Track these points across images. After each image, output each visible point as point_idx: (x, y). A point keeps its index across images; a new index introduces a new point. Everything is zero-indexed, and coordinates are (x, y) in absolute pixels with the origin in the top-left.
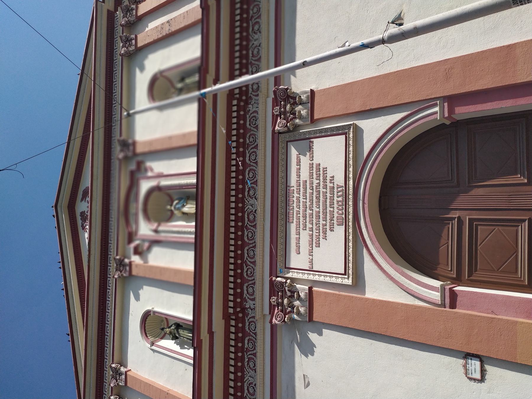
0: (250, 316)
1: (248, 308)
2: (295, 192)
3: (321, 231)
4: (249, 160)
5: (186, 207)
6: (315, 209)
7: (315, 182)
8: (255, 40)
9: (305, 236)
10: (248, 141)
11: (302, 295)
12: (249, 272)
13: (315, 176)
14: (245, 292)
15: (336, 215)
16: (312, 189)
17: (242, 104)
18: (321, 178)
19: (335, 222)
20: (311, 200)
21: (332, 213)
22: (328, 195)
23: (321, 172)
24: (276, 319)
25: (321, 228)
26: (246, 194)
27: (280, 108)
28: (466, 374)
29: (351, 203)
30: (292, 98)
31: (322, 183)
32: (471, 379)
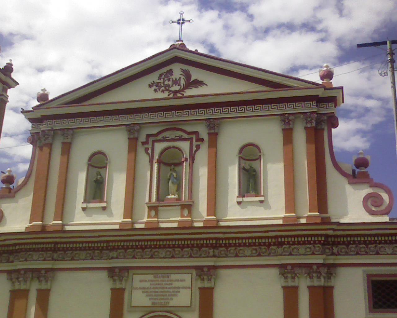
6: (159, 290)
7: (171, 290)
9: (147, 285)
14: (120, 251)
17: (214, 245)
18: (173, 293)
19: (153, 301)
20: (163, 288)
21: (157, 299)
22: (165, 297)
23: (176, 294)
29: (161, 309)
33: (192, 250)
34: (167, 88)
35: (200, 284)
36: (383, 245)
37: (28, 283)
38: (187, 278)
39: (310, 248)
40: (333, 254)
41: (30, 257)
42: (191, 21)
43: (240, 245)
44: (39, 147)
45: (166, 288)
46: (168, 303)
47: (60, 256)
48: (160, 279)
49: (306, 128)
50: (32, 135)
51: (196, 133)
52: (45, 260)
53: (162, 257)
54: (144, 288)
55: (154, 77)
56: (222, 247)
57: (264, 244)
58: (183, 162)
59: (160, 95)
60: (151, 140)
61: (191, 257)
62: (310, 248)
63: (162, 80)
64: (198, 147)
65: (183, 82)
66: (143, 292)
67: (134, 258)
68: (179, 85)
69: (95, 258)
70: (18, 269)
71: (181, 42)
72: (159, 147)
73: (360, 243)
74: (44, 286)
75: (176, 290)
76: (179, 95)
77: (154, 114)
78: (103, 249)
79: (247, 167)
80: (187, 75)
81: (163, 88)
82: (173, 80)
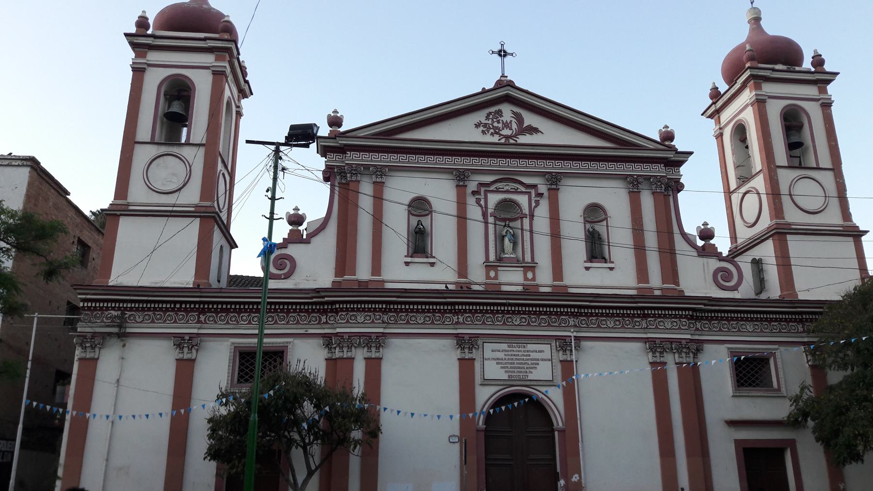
3: (505, 365)
4: (542, 318)
5: (509, 243)
6: (515, 362)
7: (529, 362)
8: (610, 322)
9: (501, 355)
10: (553, 317)
12: (479, 318)
13: (533, 362)
14: (467, 315)
15: (513, 374)
17: (575, 314)
20: (519, 359)
22: (524, 370)
23: (535, 366)
25: (506, 365)
28: (451, 436)
29: (519, 383)
33: (550, 318)
34: (497, 131)
35: (562, 357)
36: (744, 323)
37: (353, 349)
38: (546, 348)
39: (676, 322)
40: (697, 329)
42: (514, 55)
43: (602, 315)
45: (523, 360)
46: (527, 376)
47: (392, 319)
48: (514, 349)
49: (653, 193)
50: (328, 166)
51: (534, 186)
52: (373, 322)
53: (517, 324)
54: (498, 359)
55: (480, 116)
57: (628, 315)
58: (522, 218)
59: (488, 138)
60: (483, 189)
61: (549, 325)
62: (676, 322)
63: (490, 120)
64: (537, 203)
65: (514, 126)
66: (497, 363)
67: (484, 323)
68: (511, 129)
69: (435, 323)
70: (337, 333)
71: (505, 78)
72: (494, 199)
73: (722, 318)
74: (374, 355)
76: (511, 141)
78: (445, 311)
79: (591, 230)
80: (519, 119)
81: (492, 131)
82: (503, 123)
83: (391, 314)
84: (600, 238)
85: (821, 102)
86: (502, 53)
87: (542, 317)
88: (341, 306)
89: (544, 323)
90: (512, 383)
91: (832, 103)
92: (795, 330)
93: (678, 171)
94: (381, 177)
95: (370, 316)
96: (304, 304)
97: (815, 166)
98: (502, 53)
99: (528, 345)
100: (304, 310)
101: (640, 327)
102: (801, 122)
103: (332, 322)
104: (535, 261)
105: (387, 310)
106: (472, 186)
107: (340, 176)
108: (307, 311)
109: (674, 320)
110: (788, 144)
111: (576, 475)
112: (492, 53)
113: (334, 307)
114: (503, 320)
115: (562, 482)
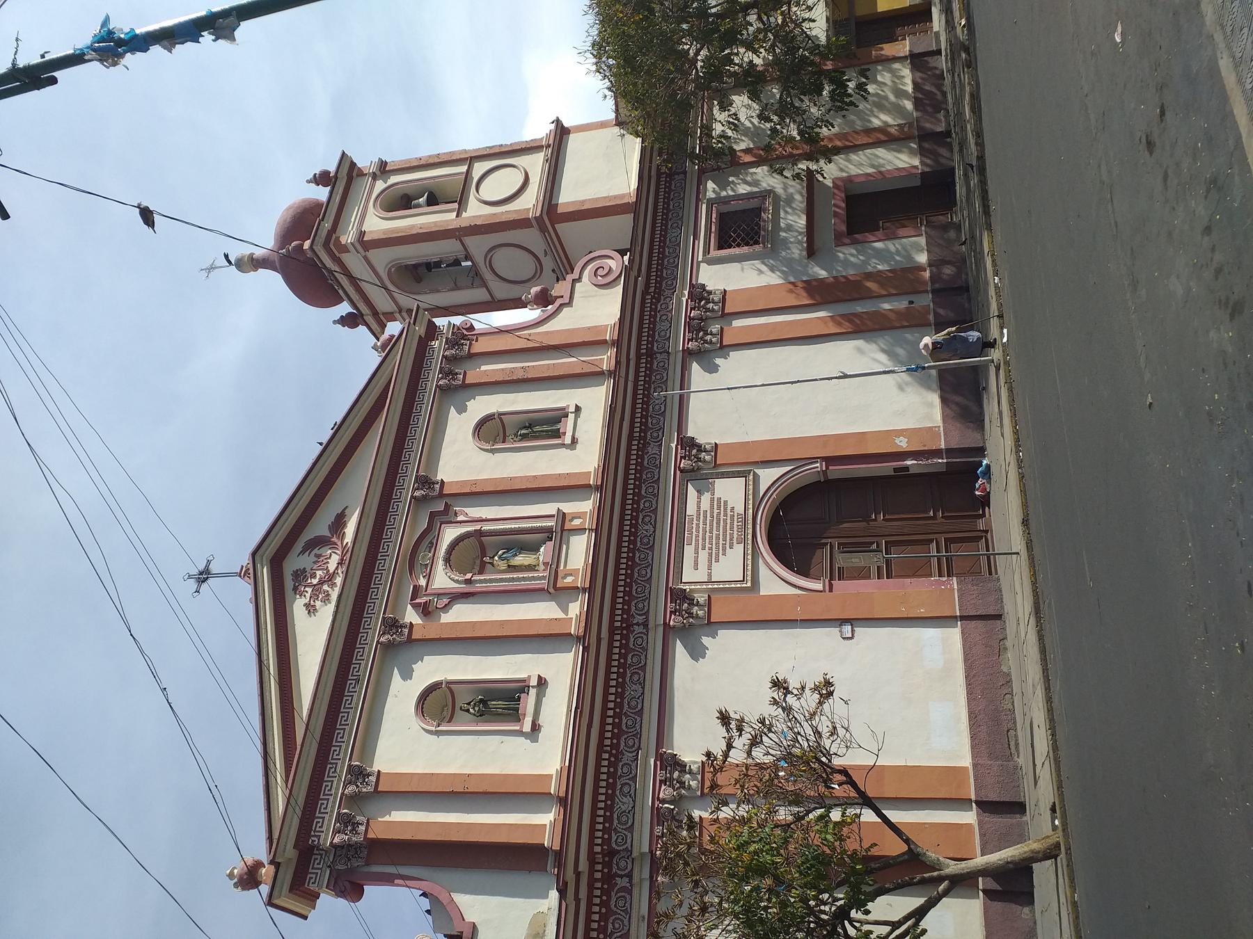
0: (635, 632)
1: (635, 624)
2: (695, 520)
6: (715, 532)
7: (716, 511)
9: (703, 555)
10: (644, 477)
11: (701, 600)
13: (715, 506)
16: (713, 517)
17: (641, 445)
18: (722, 509)
20: (711, 525)
21: (732, 535)
22: (729, 521)
24: (675, 622)
26: (640, 521)
27: (685, 452)
29: (750, 526)
30: (696, 446)
31: (722, 514)
32: (843, 638)
41: (624, 818)
42: (211, 558)
44: (368, 865)
46: (738, 514)
48: (694, 533)
49: (471, 356)
51: (433, 515)
53: (652, 529)
54: (710, 561)
56: (645, 437)
63: (307, 589)
66: (717, 561)
69: (643, 663)
70: (651, 852)
72: (443, 579)
75: (715, 503)
77: (376, 577)
83: (622, 744)
84: (530, 426)
85: (378, 173)
86: (204, 576)
87: (643, 492)
88: (599, 841)
89: (654, 489)
90: (750, 537)
91: (382, 161)
92: (681, 183)
93: (442, 328)
94: (369, 775)
95: (623, 785)
96: (588, 920)
97: (464, 176)
98: (204, 576)
99: (687, 514)
100: (602, 924)
101: (667, 361)
102: (402, 197)
103: (630, 863)
104: (554, 512)
105: (614, 752)
106: (411, 616)
107: (354, 860)
108: (604, 918)
109: (658, 319)
110: (428, 206)
111: (897, 441)
112: (198, 592)
113: (599, 858)
114: (646, 551)
115: (909, 463)
